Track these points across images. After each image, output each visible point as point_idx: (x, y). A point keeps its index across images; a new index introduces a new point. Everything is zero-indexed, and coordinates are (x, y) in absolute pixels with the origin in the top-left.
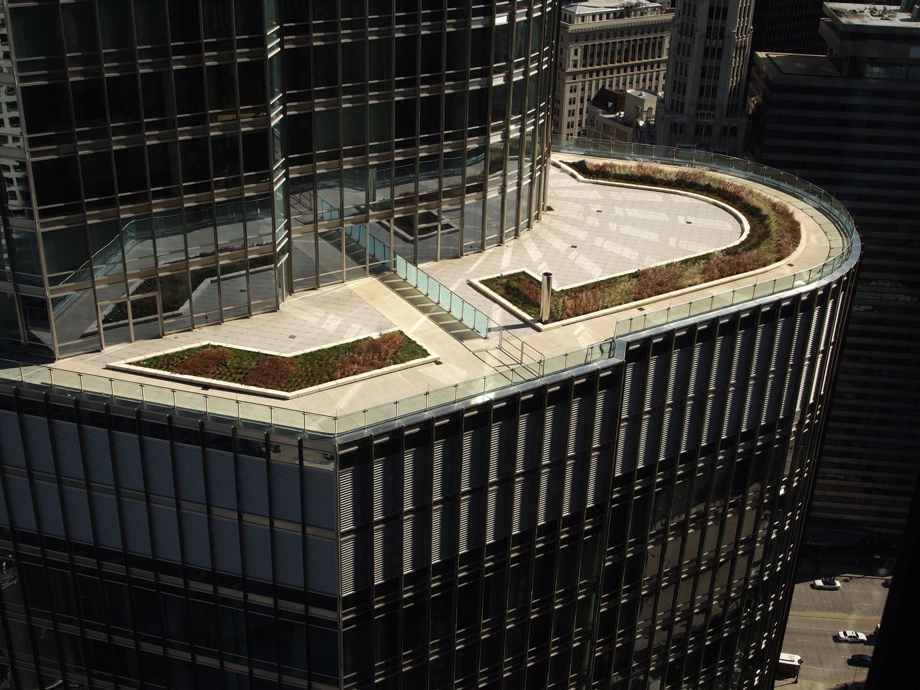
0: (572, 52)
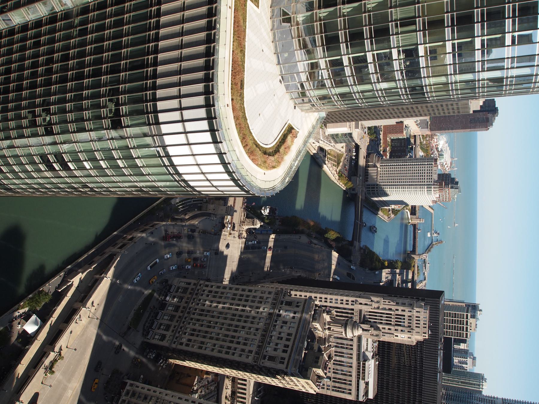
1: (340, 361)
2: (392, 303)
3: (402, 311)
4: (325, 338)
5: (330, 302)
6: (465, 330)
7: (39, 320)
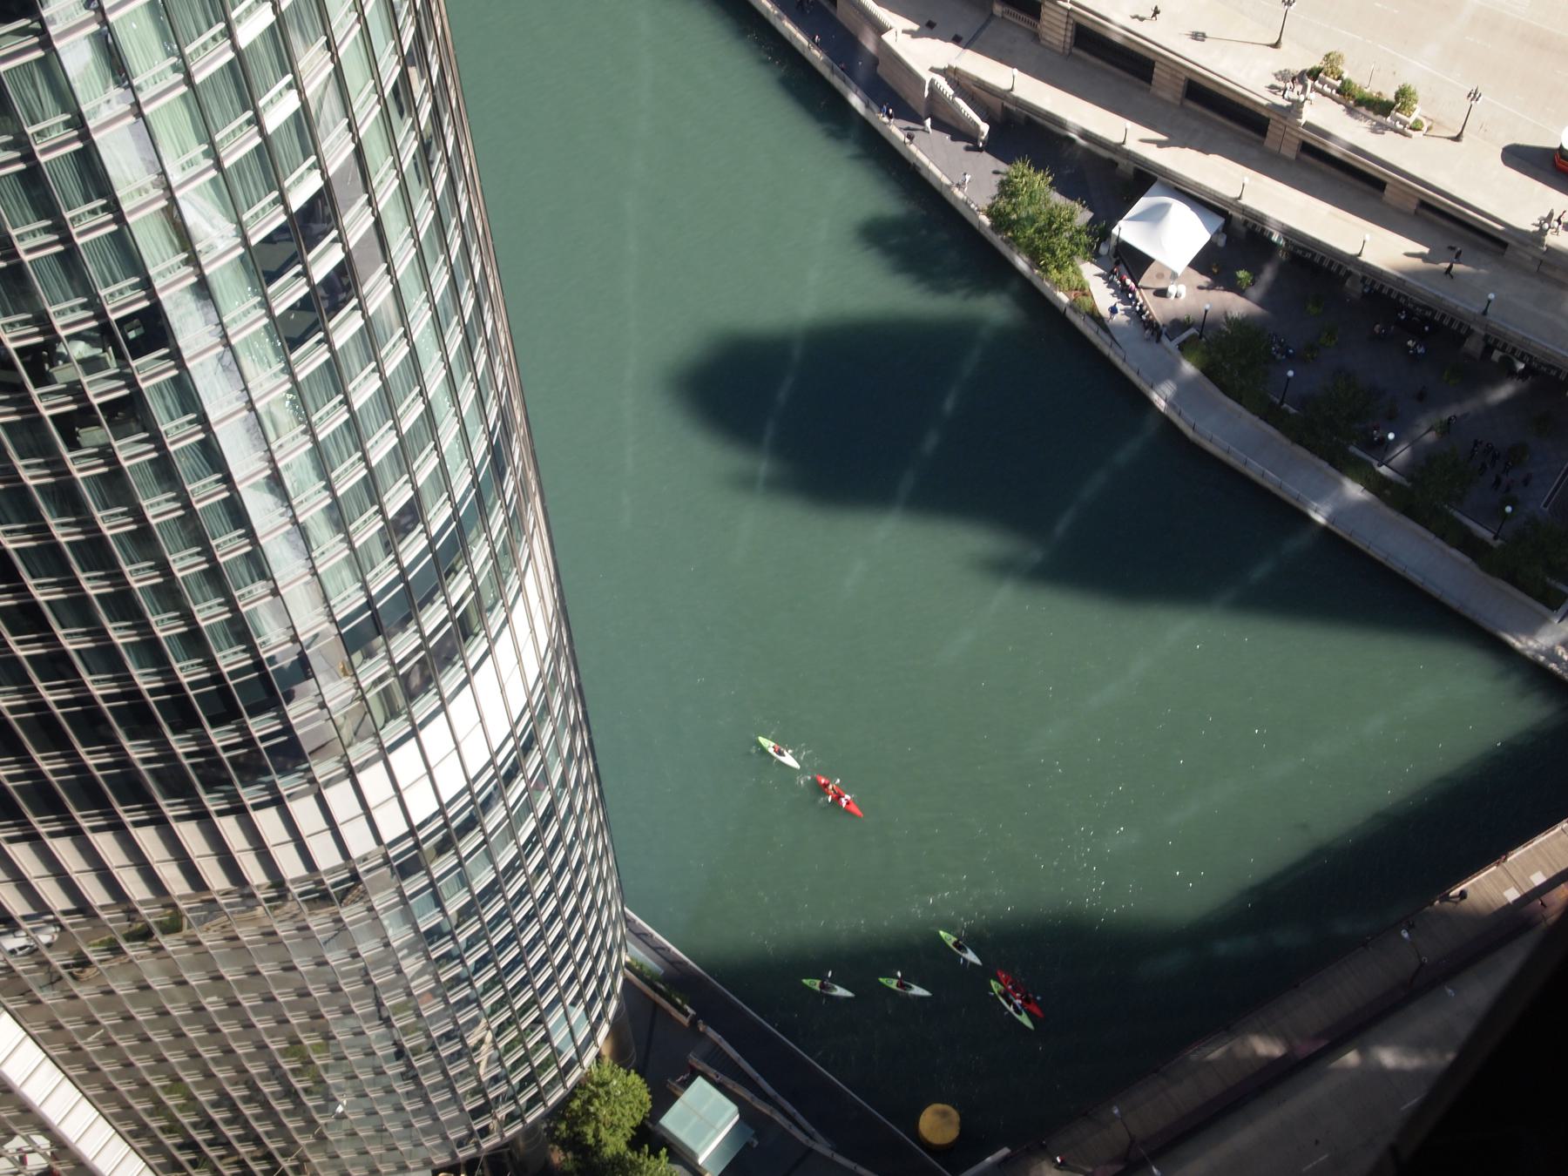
7: (1143, 203)
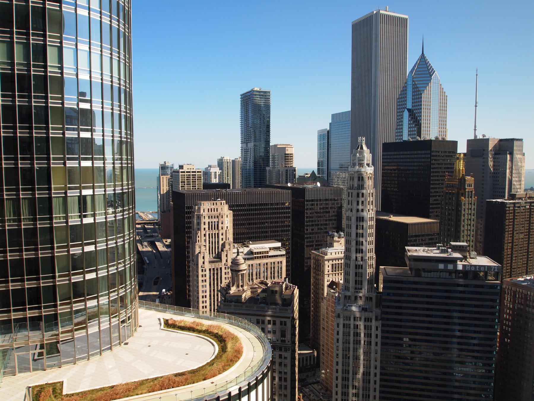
0: (327, 266)
1: (257, 275)
2: (199, 234)
3: (205, 224)
4: (251, 288)
5: (206, 292)
6: (194, 174)
